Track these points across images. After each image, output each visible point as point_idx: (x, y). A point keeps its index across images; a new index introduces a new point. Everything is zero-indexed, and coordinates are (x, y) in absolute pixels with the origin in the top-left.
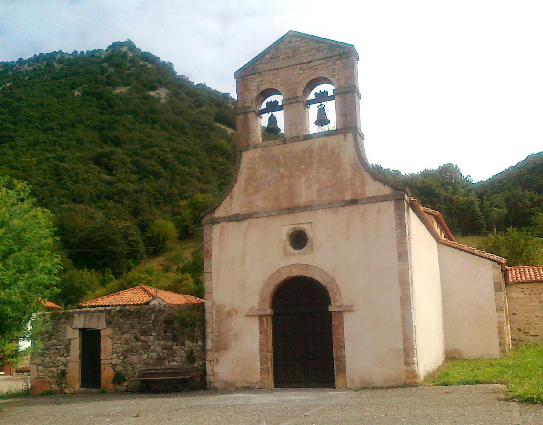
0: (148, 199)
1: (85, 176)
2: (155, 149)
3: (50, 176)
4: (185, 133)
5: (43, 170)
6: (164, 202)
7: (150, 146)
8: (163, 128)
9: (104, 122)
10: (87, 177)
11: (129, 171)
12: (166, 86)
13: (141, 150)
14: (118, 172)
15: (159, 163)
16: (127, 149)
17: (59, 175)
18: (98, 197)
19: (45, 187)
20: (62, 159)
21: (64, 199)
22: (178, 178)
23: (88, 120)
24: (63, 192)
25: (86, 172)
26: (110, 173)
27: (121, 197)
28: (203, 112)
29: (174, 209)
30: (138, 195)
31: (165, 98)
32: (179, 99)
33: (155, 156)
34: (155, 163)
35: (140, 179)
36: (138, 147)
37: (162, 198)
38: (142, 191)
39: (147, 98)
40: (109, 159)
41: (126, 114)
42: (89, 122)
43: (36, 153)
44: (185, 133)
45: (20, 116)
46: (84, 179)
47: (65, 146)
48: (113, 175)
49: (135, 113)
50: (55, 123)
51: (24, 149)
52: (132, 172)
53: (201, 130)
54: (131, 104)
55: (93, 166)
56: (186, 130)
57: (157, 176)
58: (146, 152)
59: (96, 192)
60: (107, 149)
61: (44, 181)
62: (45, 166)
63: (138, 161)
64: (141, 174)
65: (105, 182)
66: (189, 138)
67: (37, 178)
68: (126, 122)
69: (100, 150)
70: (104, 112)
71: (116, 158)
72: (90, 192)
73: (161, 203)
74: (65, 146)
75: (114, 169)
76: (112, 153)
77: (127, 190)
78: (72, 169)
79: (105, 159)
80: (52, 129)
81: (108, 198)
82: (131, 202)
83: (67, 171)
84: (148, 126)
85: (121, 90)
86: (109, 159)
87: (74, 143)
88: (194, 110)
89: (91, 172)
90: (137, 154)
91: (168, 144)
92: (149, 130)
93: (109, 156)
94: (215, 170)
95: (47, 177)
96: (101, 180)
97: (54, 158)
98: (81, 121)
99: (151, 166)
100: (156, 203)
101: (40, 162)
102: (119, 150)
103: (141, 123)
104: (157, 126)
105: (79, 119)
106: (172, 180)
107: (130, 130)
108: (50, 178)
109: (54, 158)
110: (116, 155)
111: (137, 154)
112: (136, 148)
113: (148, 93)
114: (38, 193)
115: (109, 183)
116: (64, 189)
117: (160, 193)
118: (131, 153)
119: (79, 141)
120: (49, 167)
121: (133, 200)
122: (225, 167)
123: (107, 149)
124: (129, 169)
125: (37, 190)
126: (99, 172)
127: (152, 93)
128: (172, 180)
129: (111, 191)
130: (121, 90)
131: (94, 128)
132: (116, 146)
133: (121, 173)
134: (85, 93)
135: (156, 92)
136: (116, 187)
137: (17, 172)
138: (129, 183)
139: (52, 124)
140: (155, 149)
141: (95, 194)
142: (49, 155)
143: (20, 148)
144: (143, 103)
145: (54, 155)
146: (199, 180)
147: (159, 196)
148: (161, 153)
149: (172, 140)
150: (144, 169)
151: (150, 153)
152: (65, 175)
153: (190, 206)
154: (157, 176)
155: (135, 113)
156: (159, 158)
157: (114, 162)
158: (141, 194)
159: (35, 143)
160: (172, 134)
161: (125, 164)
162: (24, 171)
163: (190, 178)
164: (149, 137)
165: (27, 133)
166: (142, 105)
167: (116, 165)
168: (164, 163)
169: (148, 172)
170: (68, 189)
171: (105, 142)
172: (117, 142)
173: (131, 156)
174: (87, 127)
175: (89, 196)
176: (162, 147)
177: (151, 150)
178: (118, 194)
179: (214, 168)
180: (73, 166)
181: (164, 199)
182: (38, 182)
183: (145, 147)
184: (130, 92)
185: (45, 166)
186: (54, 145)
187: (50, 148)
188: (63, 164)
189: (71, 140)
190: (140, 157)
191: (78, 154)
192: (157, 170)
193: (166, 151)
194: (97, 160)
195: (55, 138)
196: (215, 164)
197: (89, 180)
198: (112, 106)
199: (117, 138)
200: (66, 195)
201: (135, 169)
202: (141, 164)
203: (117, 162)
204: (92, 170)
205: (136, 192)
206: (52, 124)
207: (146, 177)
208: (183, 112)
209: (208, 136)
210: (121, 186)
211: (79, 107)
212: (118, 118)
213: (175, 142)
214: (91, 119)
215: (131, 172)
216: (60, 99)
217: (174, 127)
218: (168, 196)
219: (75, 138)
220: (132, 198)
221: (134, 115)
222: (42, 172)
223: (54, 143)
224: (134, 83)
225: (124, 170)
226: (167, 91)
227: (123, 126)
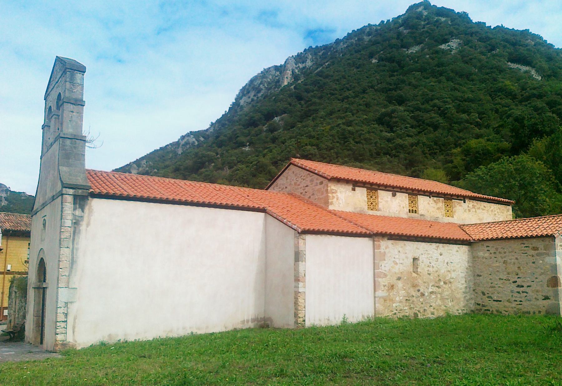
0: (423, 152)
1: (367, 136)
2: (436, 101)
3: (338, 140)
4: (473, 80)
5: (332, 136)
6: (440, 152)
7: (432, 100)
8: (448, 79)
9: (390, 84)
10: (369, 137)
11: (408, 126)
12: (457, 36)
13: (423, 104)
14: (397, 129)
15: (439, 114)
16: (409, 106)
17: (346, 138)
18: (378, 154)
19: (332, 151)
20: (349, 124)
21: (346, 159)
22: (456, 126)
23: (378, 84)
24: (346, 153)
25: (369, 132)
26: (392, 131)
27: (398, 152)
28: (493, 55)
29: (446, 157)
30: (414, 147)
31: (456, 48)
32: (471, 47)
33: (435, 108)
34: (433, 115)
35: (419, 133)
36: (419, 102)
37: (438, 147)
38: (417, 144)
39: (437, 52)
40: (391, 117)
41: (414, 72)
42: (379, 86)
43: (330, 121)
44: (473, 80)
45: (325, 91)
46: (365, 139)
47: (355, 111)
48: (393, 132)
49: (422, 70)
50: (350, 92)
51: (322, 119)
52: (412, 127)
53: (487, 74)
54: (419, 61)
55: (376, 126)
56: (474, 77)
57: (436, 127)
58: (427, 106)
59: (376, 149)
60: (391, 108)
61: (331, 145)
62: (334, 132)
63: (418, 115)
64: (421, 127)
65: (385, 139)
66: (474, 85)
67: (326, 143)
68: (413, 81)
69: (383, 110)
70: (395, 73)
71: (396, 116)
72: (370, 151)
73: (437, 152)
74: (355, 111)
75: (394, 127)
76: (393, 111)
77: (403, 144)
78: (357, 131)
79: (387, 118)
80: (347, 97)
81: (385, 154)
82: (407, 155)
83: (353, 134)
84: (434, 80)
85: (414, 49)
86: (391, 117)
87: (362, 107)
88: (485, 55)
89: (373, 132)
90: (419, 109)
91: (451, 94)
92: (432, 83)
93: (389, 115)
94: (497, 113)
95: (335, 141)
96: (381, 138)
97: (343, 124)
98: (372, 87)
99: (431, 118)
100: (432, 153)
101: (332, 129)
102: (401, 108)
103: (428, 78)
104: (443, 78)
105: (370, 85)
106: (450, 129)
107: (416, 87)
108: (338, 142)
109: (343, 124)
110: (396, 113)
111: (419, 109)
112: (417, 104)
113: (440, 47)
114: (326, 156)
115: (389, 140)
116: (348, 150)
117: (436, 144)
118: (412, 109)
119: (367, 105)
120: (337, 133)
121: (408, 154)
122: (507, 109)
123: (391, 108)
124: (409, 124)
125: (326, 154)
126: (381, 131)
127: (443, 47)
128: (450, 129)
129: (390, 147)
130: (414, 49)
131: (383, 91)
132: (400, 105)
133: (401, 129)
134: (381, 59)
135: (447, 44)
136: (394, 142)
137: (312, 140)
138: (407, 138)
139: (347, 93)
140: (436, 101)
141: (375, 151)
142: (340, 121)
143: (319, 119)
144: (433, 59)
145: (344, 121)
146: (478, 125)
147: (435, 147)
148: (441, 104)
149: (456, 89)
150: (423, 122)
151: (431, 106)
152: (350, 137)
153: (462, 152)
154: (436, 127)
155: (422, 70)
156: (439, 109)
157: (394, 120)
158: (416, 146)
159: (331, 113)
160: (458, 84)
161: (404, 120)
162: (318, 139)
163: (468, 125)
164: (432, 91)
165: (328, 104)
166: (431, 61)
167: (396, 122)
168: (443, 114)
169: (428, 125)
170: (350, 150)
171: (390, 102)
172: (401, 101)
173: (413, 112)
174: (376, 90)
175: (368, 154)
176: (443, 98)
177: (431, 103)
178: (396, 149)
179: (497, 111)
180: (358, 128)
181: (440, 147)
182: (326, 147)
183: (427, 102)
184: (423, 49)
185: (334, 132)
186: (346, 112)
187: (343, 115)
188: (349, 128)
189: (360, 105)
190: (420, 112)
191: (365, 117)
192: (436, 122)
193: (447, 102)
194: (380, 121)
195: (347, 106)
196: (498, 107)
197: (371, 139)
198: (402, 67)
199: (401, 96)
200: (349, 155)
201: (415, 123)
202: (421, 118)
203: (397, 120)
204: (374, 130)
205: (412, 145)
206: (347, 93)
207: (425, 129)
208: (471, 59)
209: (495, 80)
210: (399, 141)
211: (374, 74)
212: (405, 78)
213: (459, 91)
214: (381, 83)
215: (410, 127)
216: (359, 70)
217: (461, 76)
218: (444, 145)
219: (364, 103)
220: (407, 152)
221: (422, 72)
222: (331, 137)
223: (346, 110)
224: (426, 40)
225: (403, 126)
226: (459, 41)
227: (410, 84)
